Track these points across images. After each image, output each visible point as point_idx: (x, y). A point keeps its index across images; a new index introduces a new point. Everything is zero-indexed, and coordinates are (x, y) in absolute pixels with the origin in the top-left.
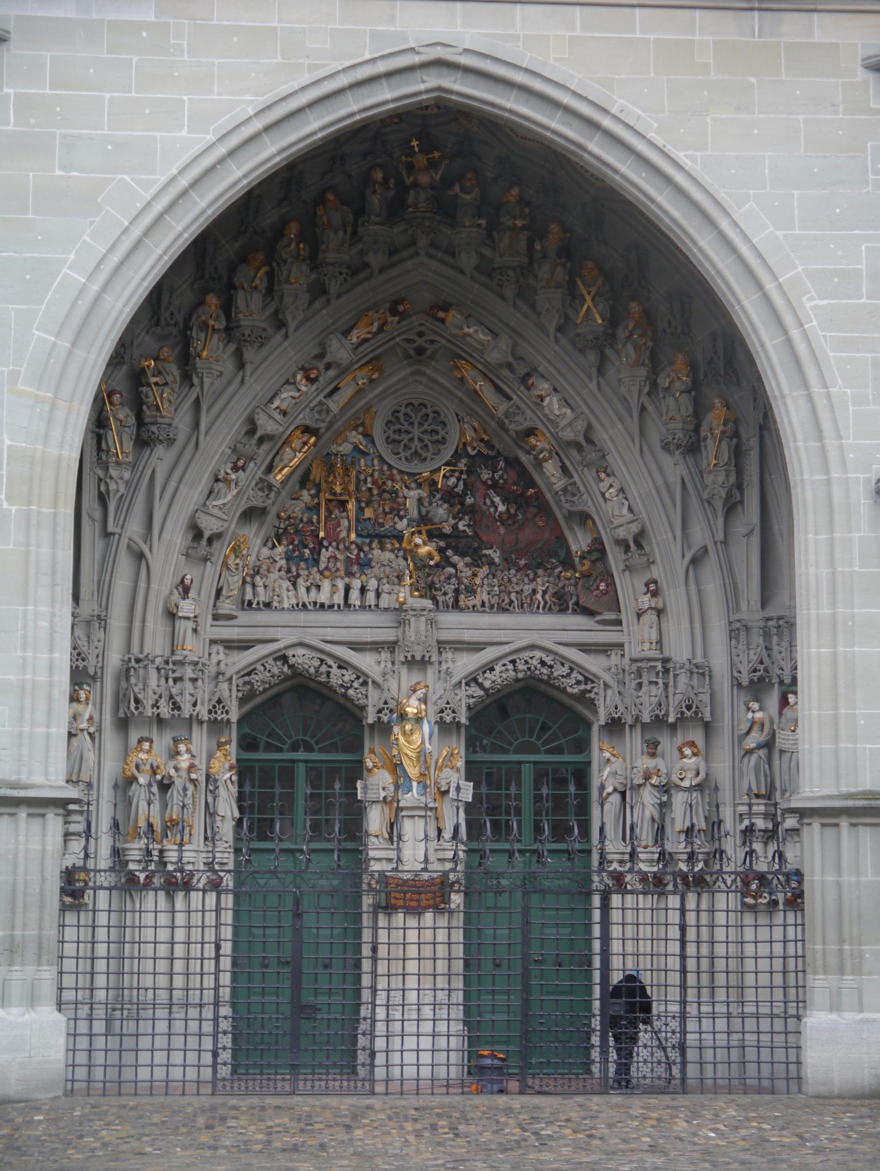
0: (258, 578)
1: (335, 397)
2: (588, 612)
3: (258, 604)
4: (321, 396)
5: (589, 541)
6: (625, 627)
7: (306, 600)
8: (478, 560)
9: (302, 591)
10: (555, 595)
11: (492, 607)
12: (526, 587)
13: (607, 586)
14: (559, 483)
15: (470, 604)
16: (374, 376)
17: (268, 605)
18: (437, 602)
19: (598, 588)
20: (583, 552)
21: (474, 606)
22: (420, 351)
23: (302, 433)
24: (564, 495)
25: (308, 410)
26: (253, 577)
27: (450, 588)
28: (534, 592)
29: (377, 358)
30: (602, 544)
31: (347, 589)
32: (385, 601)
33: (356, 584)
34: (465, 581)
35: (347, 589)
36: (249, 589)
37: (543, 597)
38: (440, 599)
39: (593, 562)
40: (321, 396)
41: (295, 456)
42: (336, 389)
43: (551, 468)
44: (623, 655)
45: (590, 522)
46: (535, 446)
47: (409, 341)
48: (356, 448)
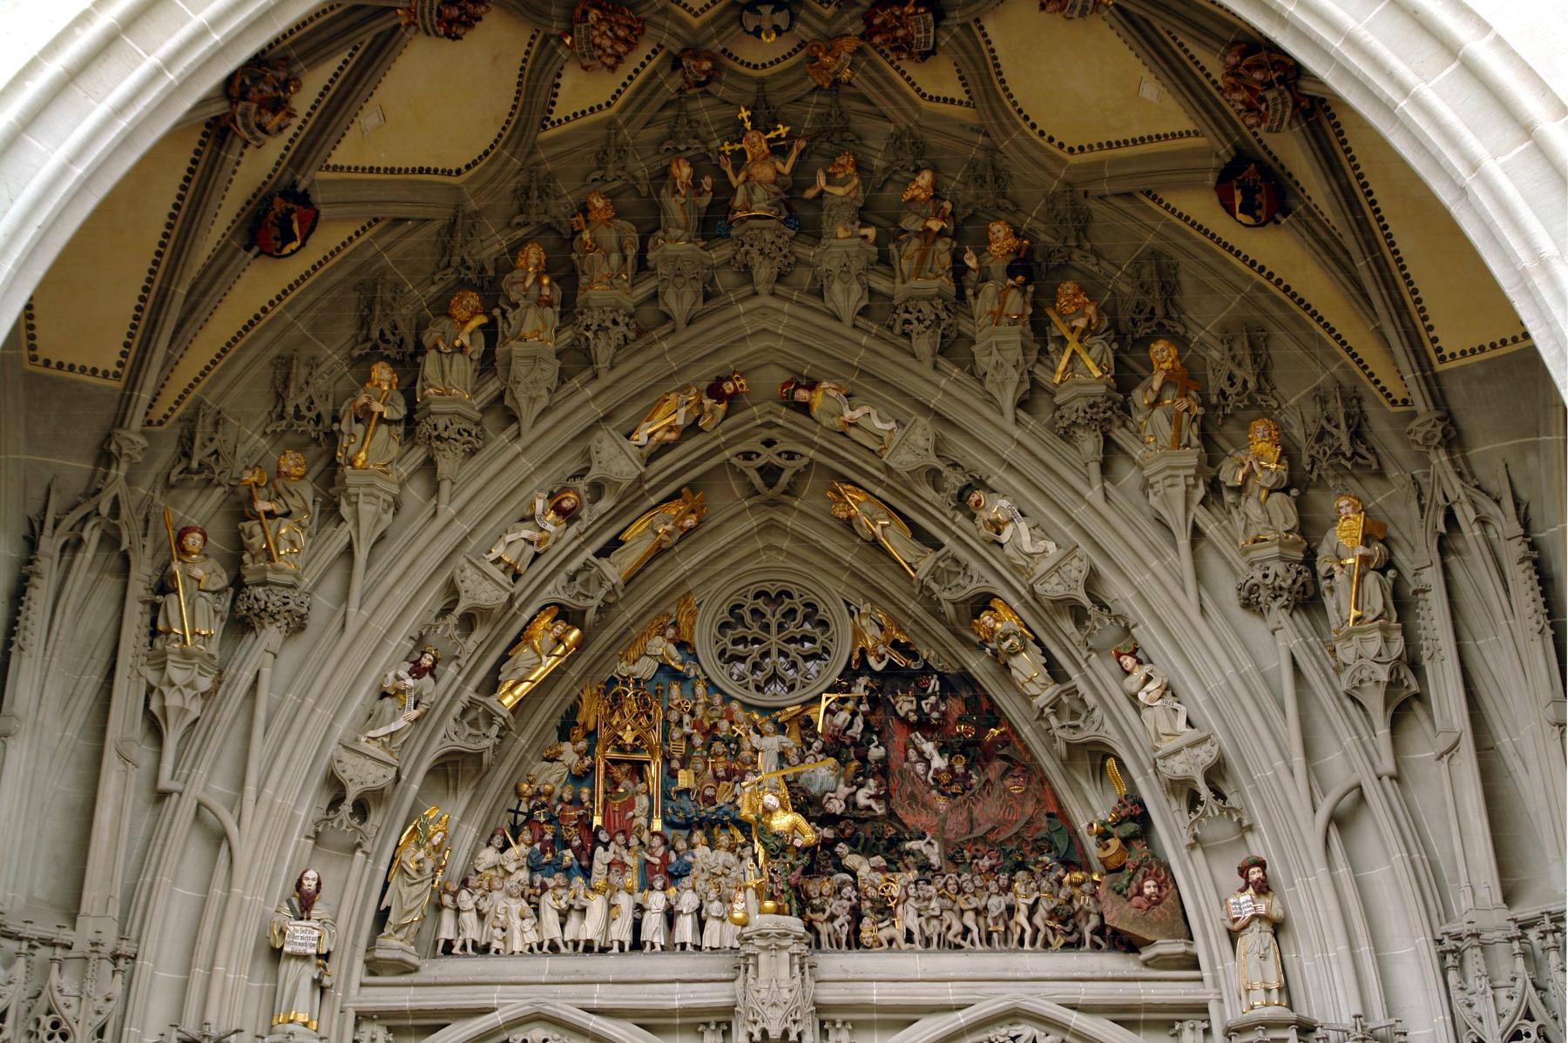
0: (464, 893)
1: (614, 557)
2: (1126, 944)
3: (464, 947)
4: (588, 553)
5: (1113, 801)
6: (1205, 971)
7: (556, 933)
8: (892, 852)
9: (550, 918)
10: (1053, 914)
11: (928, 942)
12: (994, 901)
13: (1159, 887)
14: (1044, 693)
15: (884, 935)
16: (690, 522)
17: (483, 950)
18: (818, 934)
19: (1140, 892)
20: (1104, 824)
21: (891, 941)
22: (770, 473)
23: (554, 620)
24: (1055, 714)
25: (562, 578)
26: (455, 895)
27: (840, 907)
28: (1011, 910)
29: (693, 486)
30: (1141, 804)
31: (640, 908)
32: (714, 933)
33: (657, 901)
34: (872, 893)
35: (640, 908)
36: (447, 917)
37: (1030, 919)
38: (824, 929)
39: (1126, 841)
40: (588, 553)
41: (540, 664)
42: (616, 543)
43: (1027, 665)
44: (1207, 1032)
45: (1111, 763)
46: (993, 631)
47: (747, 456)
48: (663, 667)
